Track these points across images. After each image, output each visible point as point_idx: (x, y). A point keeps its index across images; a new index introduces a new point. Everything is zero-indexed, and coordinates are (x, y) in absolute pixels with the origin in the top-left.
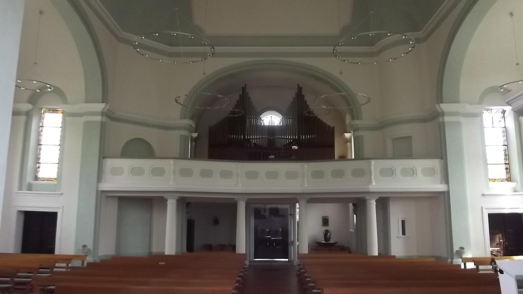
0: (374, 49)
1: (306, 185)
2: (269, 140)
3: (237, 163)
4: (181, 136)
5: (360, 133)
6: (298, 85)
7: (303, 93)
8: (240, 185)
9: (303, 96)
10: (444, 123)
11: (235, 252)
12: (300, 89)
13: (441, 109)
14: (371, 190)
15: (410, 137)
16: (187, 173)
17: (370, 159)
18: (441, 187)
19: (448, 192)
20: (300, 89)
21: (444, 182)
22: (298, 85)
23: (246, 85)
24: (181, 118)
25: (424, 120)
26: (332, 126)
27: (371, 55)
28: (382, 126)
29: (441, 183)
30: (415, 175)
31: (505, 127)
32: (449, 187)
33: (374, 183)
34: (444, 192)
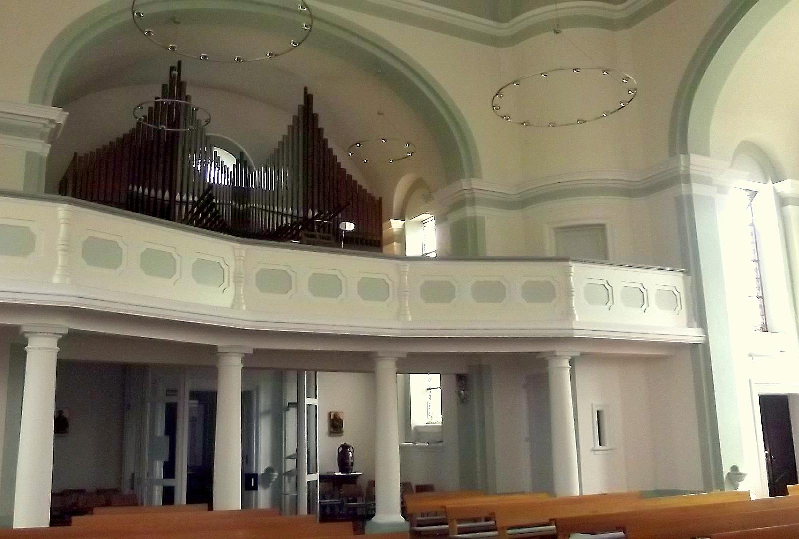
0: (504, 30)
1: (410, 319)
2: (235, 211)
3: (238, 245)
4: (30, 156)
5: (480, 211)
6: (306, 89)
7: (315, 110)
8: (244, 307)
9: (315, 118)
10: (690, 197)
11: (211, 508)
12: (308, 99)
13: (687, 167)
14: (577, 334)
15: (602, 227)
16: (101, 253)
17: (566, 259)
18: (693, 335)
19: (705, 346)
20: (308, 99)
21: (695, 324)
22: (306, 89)
23: (180, 63)
24: (33, 100)
25: (629, 191)
26: (377, 198)
27: (495, 41)
28: (523, 202)
29: (689, 325)
30: (645, 306)
31: (752, 225)
32: (706, 333)
33: (577, 319)
34: (693, 347)
